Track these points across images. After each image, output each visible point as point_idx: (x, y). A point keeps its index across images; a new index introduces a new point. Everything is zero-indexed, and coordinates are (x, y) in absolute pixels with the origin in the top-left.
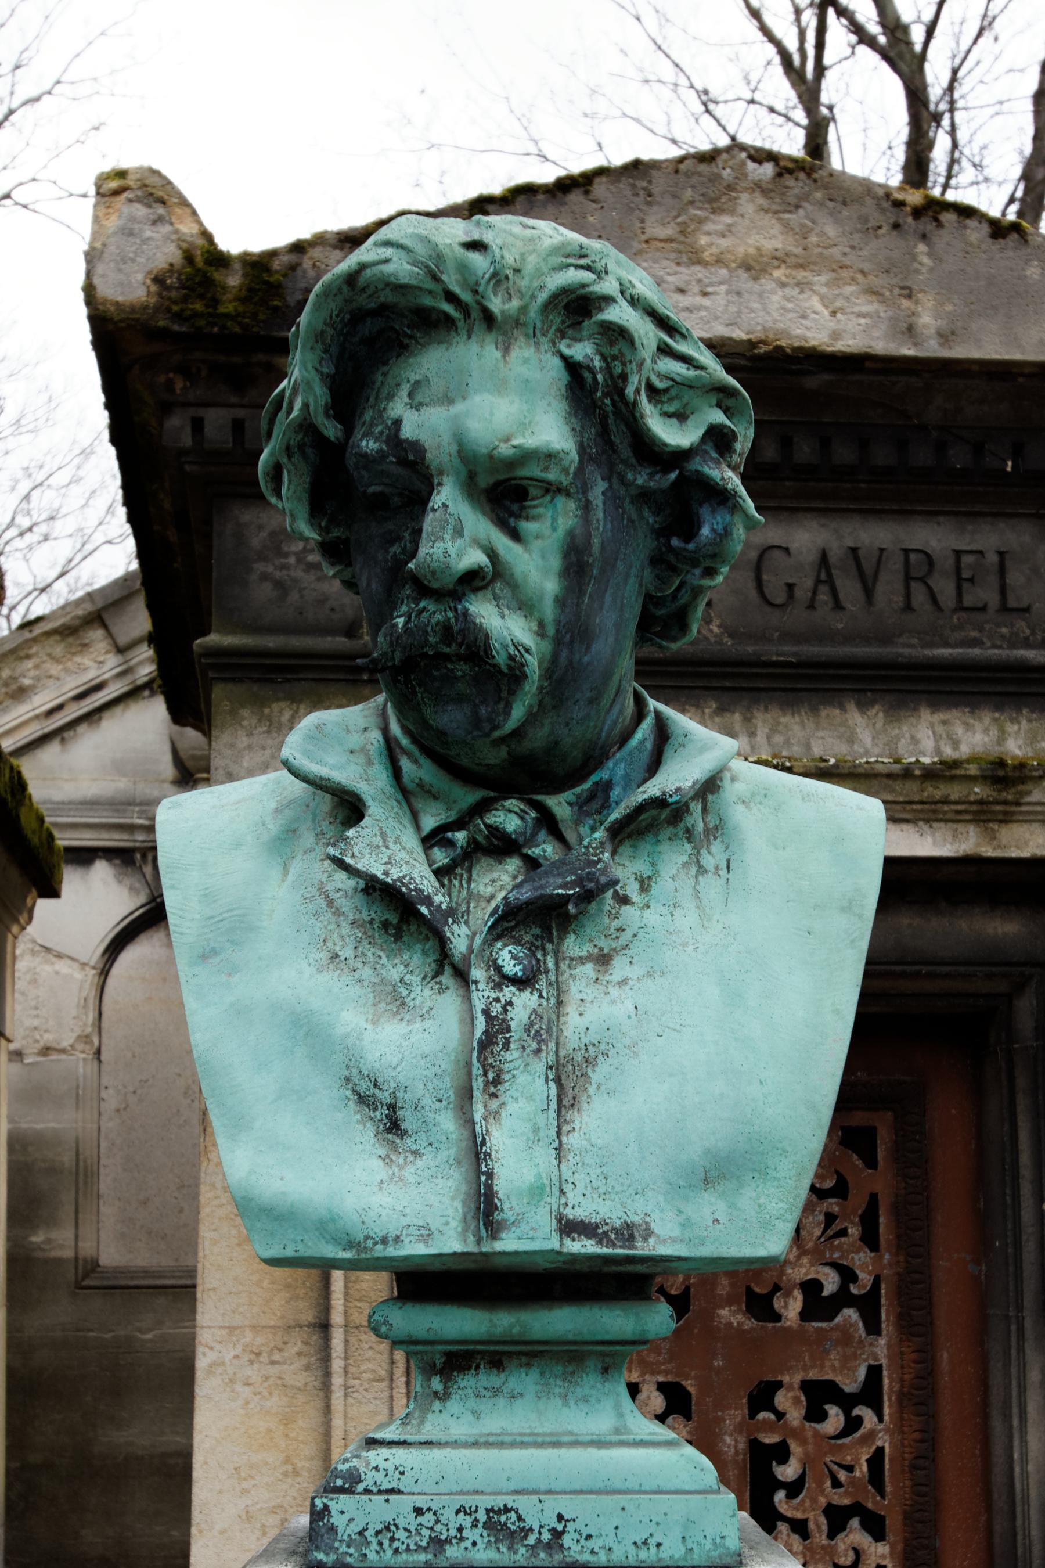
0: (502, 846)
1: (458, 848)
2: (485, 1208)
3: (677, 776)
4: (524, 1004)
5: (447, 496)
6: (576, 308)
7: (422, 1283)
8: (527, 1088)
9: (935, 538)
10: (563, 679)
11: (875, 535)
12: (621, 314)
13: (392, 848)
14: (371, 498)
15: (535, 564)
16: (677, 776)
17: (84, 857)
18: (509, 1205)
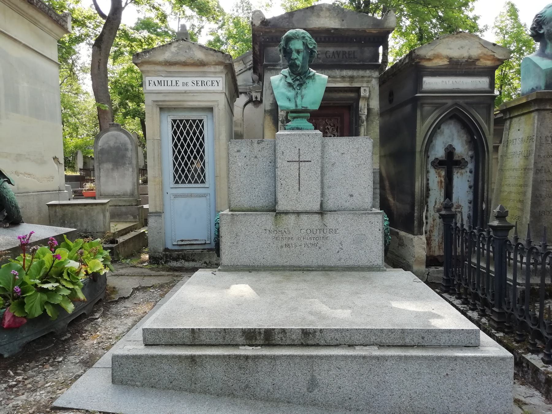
0: (298, 80)
1: (295, 80)
2: (296, 106)
3: (311, 74)
4: (299, 91)
5: (294, 52)
6: (304, 37)
7: (293, 112)
8: (299, 97)
9: (346, 49)
10: (302, 67)
11: (339, 49)
12: (307, 38)
13: (290, 80)
14: (287, 52)
15: (300, 57)
16: (311, 74)
17: (241, 93)
18: (298, 105)
